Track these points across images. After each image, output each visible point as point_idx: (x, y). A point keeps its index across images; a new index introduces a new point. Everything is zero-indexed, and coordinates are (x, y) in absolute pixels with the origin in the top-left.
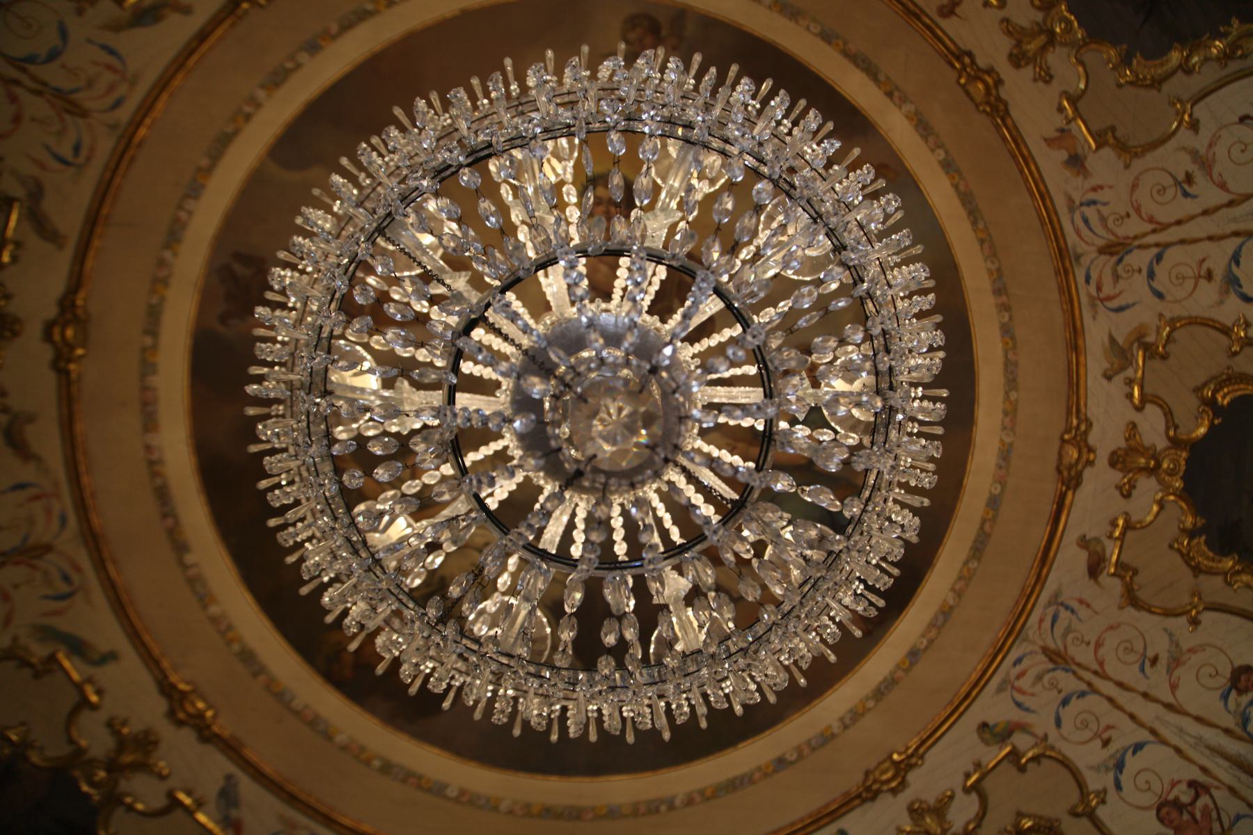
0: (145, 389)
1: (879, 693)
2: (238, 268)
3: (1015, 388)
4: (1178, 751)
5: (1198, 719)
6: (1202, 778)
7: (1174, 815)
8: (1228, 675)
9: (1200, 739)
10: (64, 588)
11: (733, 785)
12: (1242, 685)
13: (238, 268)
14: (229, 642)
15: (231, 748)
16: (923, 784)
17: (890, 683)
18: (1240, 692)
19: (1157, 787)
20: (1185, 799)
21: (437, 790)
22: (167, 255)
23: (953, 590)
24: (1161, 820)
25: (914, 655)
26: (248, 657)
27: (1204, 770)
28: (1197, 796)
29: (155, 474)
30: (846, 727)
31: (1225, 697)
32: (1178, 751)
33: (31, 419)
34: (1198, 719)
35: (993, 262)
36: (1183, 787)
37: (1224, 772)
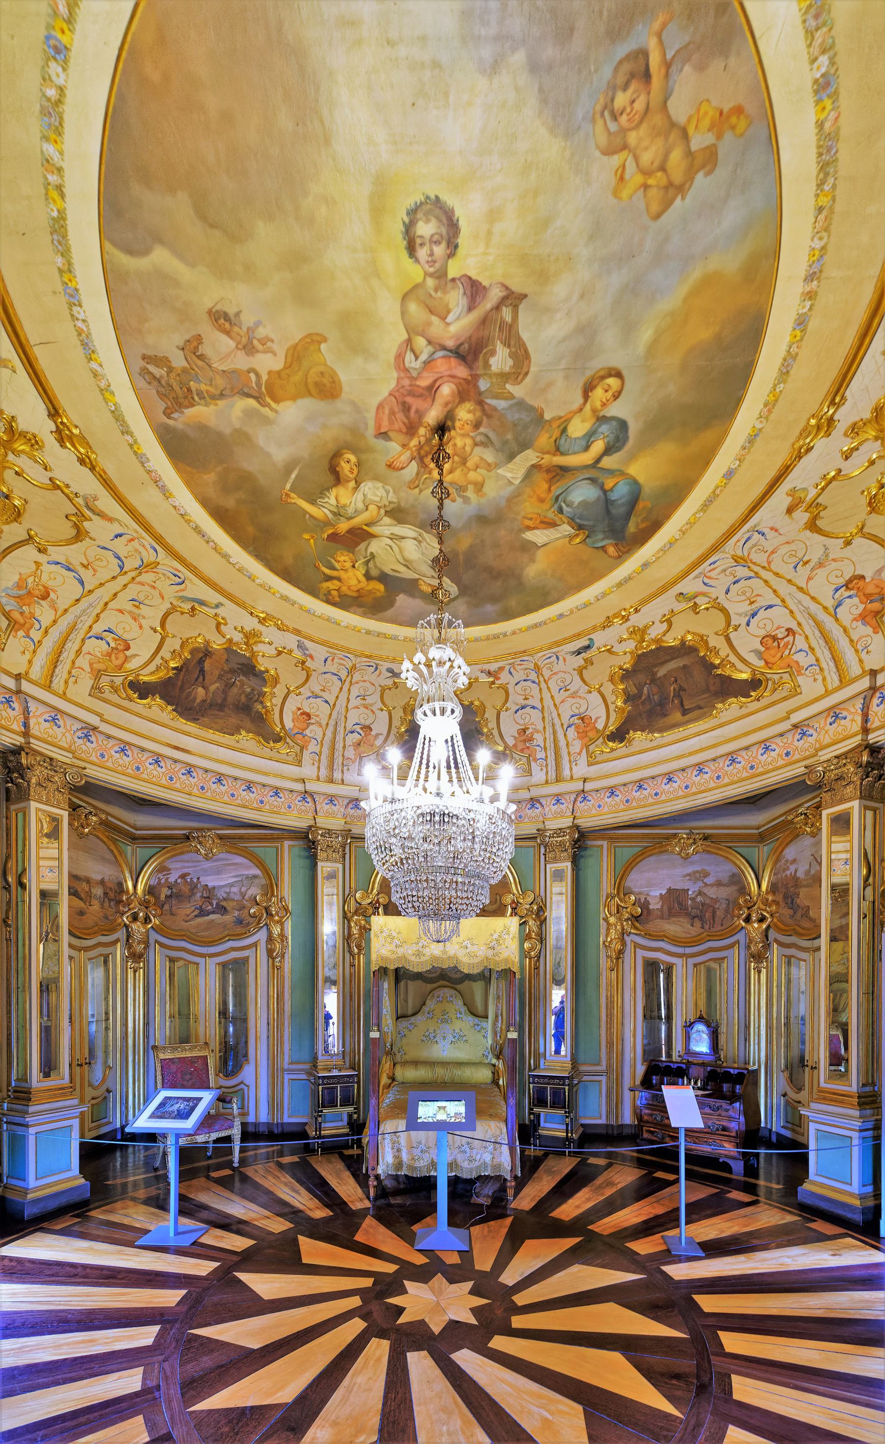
0: (149, 472)
1: (620, 585)
2: (151, 368)
3: (784, 382)
4: (791, 612)
5: (813, 598)
6: (795, 627)
7: (770, 641)
8: (847, 578)
9: (807, 608)
10: (178, 580)
11: (536, 626)
12: (850, 586)
13: (151, 368)
14: (274, 594)
15: (297, 632)
16: (637, 620)
17: (628, 579)
18: (847, 588)
19: (768, 628)
20: (780, 636)
21: (395, 638)
22: (94, 365)
23: (681, 530)
24: (761, 643)
25: (645, 565)
26: (285, 598)
27: (799, 624)
28: (788, 635)
29: (188, 522)
30: (598, 600)
31: (837, 590)
32: (791, 612)
33: (95, 499)
34: (813, 598)
35: (821, 239)
36: (783, 630)
37: (809, 628)
